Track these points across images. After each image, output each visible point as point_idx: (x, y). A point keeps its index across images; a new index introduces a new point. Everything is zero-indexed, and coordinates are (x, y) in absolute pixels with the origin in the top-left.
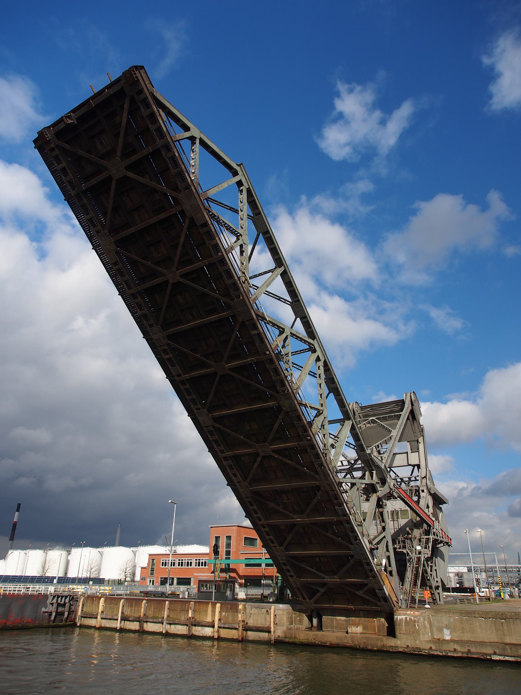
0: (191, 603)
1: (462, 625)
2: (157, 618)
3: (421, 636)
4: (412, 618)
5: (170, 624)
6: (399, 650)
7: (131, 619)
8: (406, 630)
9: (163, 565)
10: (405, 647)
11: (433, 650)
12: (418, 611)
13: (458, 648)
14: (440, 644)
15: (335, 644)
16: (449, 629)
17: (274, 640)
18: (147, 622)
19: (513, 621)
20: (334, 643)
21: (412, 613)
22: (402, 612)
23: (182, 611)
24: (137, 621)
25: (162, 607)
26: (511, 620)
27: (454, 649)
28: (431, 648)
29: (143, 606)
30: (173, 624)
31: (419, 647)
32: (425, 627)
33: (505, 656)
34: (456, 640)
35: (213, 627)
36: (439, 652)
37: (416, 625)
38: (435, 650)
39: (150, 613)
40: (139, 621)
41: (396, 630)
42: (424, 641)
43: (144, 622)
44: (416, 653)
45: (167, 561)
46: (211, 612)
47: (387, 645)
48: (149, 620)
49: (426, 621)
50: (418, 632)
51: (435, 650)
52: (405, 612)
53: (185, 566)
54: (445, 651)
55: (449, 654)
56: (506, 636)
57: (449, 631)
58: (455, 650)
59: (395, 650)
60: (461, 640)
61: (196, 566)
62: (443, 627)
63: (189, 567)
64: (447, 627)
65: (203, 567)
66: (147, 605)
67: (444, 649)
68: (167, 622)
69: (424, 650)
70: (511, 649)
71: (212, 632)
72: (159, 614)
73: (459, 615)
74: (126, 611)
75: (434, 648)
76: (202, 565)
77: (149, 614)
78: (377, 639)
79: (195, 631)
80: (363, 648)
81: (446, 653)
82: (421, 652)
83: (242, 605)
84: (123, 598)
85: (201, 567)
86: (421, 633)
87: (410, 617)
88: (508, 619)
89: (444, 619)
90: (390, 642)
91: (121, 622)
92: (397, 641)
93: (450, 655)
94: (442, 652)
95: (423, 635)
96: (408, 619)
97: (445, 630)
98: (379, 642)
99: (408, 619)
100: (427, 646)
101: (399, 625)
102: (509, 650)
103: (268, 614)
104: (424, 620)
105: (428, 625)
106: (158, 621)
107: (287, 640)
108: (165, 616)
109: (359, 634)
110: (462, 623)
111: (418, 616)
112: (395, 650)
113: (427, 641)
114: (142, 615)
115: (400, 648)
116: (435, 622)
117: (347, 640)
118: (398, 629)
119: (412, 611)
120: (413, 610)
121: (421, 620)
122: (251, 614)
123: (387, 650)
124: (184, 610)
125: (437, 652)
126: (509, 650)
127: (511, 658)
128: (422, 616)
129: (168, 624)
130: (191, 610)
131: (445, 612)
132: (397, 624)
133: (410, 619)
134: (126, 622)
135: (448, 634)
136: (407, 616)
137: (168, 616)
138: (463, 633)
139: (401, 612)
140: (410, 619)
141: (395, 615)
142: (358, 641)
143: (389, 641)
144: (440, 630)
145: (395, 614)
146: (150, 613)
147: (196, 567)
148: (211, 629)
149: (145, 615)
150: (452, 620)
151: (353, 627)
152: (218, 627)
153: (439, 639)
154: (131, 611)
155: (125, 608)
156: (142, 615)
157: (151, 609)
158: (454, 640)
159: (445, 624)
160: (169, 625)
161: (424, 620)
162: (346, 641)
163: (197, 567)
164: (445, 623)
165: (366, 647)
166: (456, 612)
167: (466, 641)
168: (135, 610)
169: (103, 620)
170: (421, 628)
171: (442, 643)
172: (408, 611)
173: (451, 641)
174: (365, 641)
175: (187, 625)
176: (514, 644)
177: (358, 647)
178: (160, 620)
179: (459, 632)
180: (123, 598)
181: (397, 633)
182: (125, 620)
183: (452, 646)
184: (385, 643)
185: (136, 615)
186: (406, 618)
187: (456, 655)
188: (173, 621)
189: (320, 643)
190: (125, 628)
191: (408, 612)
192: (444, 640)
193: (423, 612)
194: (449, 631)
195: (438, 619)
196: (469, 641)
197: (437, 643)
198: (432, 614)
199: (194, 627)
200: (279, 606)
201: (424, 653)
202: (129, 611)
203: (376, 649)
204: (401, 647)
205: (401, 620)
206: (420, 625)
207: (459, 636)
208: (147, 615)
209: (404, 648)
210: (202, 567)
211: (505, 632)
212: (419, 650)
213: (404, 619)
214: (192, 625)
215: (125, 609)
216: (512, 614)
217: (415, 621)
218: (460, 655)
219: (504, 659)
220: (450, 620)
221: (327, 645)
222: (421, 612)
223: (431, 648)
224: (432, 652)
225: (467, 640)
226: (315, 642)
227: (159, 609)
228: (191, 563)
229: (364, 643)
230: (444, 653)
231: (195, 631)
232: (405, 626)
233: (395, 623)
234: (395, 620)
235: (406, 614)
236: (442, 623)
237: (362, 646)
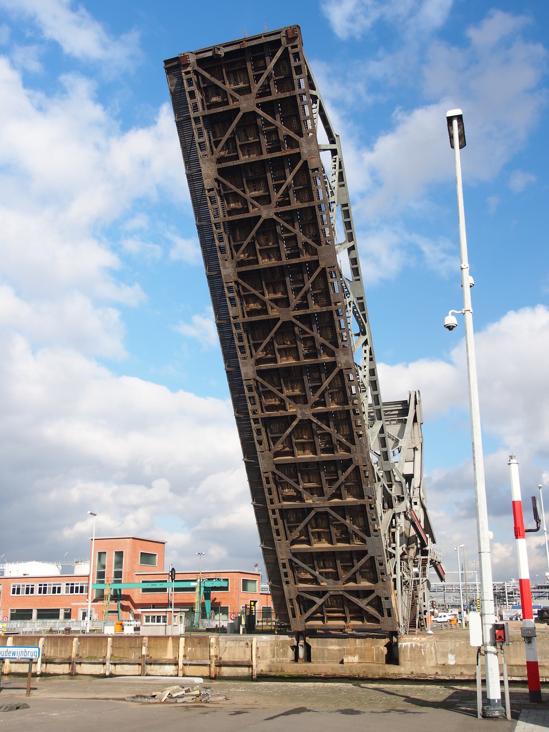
0: (144, 638)
1: (468, 649)
2: (96, 658)
3: (427, 662)
4: (418, 644)
5: (115, 664)
6: (403, 677)
7: (57, 661)
8: (411, 657)
9: (14, 593)
10: (409, 673)
11: (439, 675)
12: (425, 637)
13: (465, 672)
14: (447, 668)
15: (331, 675)
16: (454, 654)
17: (257, 674)
18: (80, 663)
19: (520, 643)
20: (329, 673)
21: (418, 639)
22: (407, 638)
23: (131, 648)
24: (65, 663)
25: (101, 645)
26: (518, 642)
27: (461, 673)
28: (437, 673)
29: (74, 644)
30: (118, 664)
31: (424, 673)
32: (431, 653)
33: (512, 676)
34: (460, 665)
35: (176, 664)
36: (446, 676)
37: (422, 651)
38: (441, 675)
39: (85, 652)
40: (70, 663)
41: (400, 656)
42: (430, 667)
43: (77, 663)
44: (421, 678)
45: (21, 587)
46: (172, 648)
47: (390, 673)
48: (84, 661)
49: (432, 647)
50: (424, 658)
51: (441, 675)
52: (411, 639)
53: (23, 593)
54: (452, 675)
55: (456, 678)
56: (512, 659)
57: (454, 655)
58: (462, 674)
59: (399, 677)
60: (466, 665)
61: (67, 592)
62: (447, 653)
63: (57, 594)
64: (452, 652)
65: (79, 593)
66: (79, 643)
67: (450, 674)
68: (112, 662)
69: (430, 675)
70: (518, 669)
71: (174, 671)
72: (97, 653)
73: (465, 640)
74: (47, 651)
75: (439, 673)
76: (77, 592)
77: (83, 654)
78: (379, 668)
79: (151, 670)
80: (363, 677)
81: (453, 677)
82: (426, 677)
83: (214, 639)
84: (42, 637)
85: (74, 594)
86: (427, 659)
87: (416, 643)
88: (515, 642)
89: (449, 644)
90: (392, 670)
91: (41, 666)
92: (401, 668)
93: (457, 678)
94: (449, 677)
95: (429, 661)
96: (414, 645)
97: (450, 655)
98: (381, 671)
99: (414, 645)
100: (433, 672)
101: (404, 652)
102: (516, 671)
103: (247, 647)
104: (431, 646)
105: (433, 651)
106: (98, 662)
107: (273, 674)
108: (109, 655)
109: (356, 663)
110: (468, 648)
111: (424, 642)
112: (399, 677)
113: (433, 667)
114: (73, 656)
115: (404, 675)
116: (440, 647)
117: (344, 671)
118: (402, 656)
119: (418, 637)
120: (419, 636)
121: (428, 646)
122: (226, 648)
123: (390, 677)
124: (133, 647)
125: (444, 676)
126: (516, 671)
127: (518, 678)
128: (429, 642)
129: (111, 664)
130: (145, 646)
131: (451, 637)
132: (402, 651)
133: (416, 646)
134: (48, 665)
135: (453, 659)
136: (412, 643)
137: (112, 655)
138: (468, 657)
139: (406, 638)
140: (416, 646)
141: (400, 642)
142: (357, 671)
143: (392, 668)
144: (445, 655)
145: (400, 641)
146: (85, 652)
147: (67, 594)
148: (173, 667)
149: (77, 655)
150: (457, 644)
151: (349, 656)
152: (183, 664)
153: (444, 665)
154: (55, 651)
155: (46, 648)
156: (73, 656)
157: (85, 648)
158: (458, 665)
159: (450, 649)
160: (113, 666)
161: (431, 646)
162: (343, 672)
163: (69, 594)
164: (450, 648)
165: (366, 676)
166: (462, 637)
167: (471, 665)
168: (61, 651)
169: (13, 665)
170: (427, 654)
171: (449, 668)
172: (414, 637)
173: (456, 666)
174: (365, 670)
175: (139, 664)
176: (519, 666)
177: (357, 676)
178: (101, 660)
179: (464, 657)
180: (42, 637)
181: (401, 660)
182: (46, 663)
183: (458, 671)
184: (387, 671)
185: (65, 656)
186: (412, 645)
187: (463, 679)
188: (120, 660)
189: (313, 675)
190: (48, 672)
191: (414, 639)
192: (449, 665)
193: (430, 638)
194: (454, 655)
195: (443, 645)
196: (474, 665)
197: (444, 668)
198: (437, 640)
199: (149, 666)
200: (263, 638)
201: (430, 679)
202: (52, 651)
203: (377, 677)
204: (405, 674)
205: (406, 647)
206: (426, 651)
207: (464, 660)
208: (80, 655)
209: (408, 674)
210: (77, 594)
211: (511, 654)
212: (424, 676)
213: (409, 646)
214: (147, 664)
215: (46, 650)
216: (519, 636)
217: (421, 647)
218: (467, 678)
219: (511, 679)
220: (455, 645)
221: (321, 677)
222: (428, 638)
223: (437, 673)
224: (438, 677)
225: (472, 664)
226: (307, 675)
227: (98, 647)
228: (59, 588)
229: (364, 672)
230: (451, 678)
231: (151, 670)
232: (410, 652)
233: (399, 651)
234: (399, 646)
235: (412, 641)
236: (447, 648)
237: (362, 675)
